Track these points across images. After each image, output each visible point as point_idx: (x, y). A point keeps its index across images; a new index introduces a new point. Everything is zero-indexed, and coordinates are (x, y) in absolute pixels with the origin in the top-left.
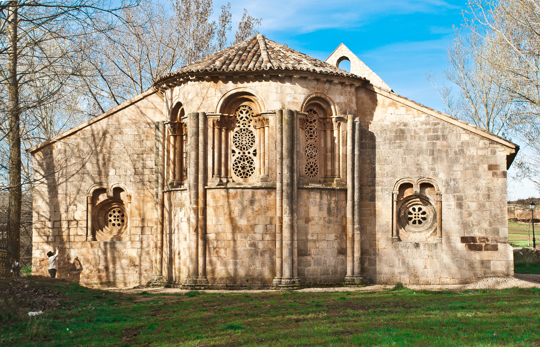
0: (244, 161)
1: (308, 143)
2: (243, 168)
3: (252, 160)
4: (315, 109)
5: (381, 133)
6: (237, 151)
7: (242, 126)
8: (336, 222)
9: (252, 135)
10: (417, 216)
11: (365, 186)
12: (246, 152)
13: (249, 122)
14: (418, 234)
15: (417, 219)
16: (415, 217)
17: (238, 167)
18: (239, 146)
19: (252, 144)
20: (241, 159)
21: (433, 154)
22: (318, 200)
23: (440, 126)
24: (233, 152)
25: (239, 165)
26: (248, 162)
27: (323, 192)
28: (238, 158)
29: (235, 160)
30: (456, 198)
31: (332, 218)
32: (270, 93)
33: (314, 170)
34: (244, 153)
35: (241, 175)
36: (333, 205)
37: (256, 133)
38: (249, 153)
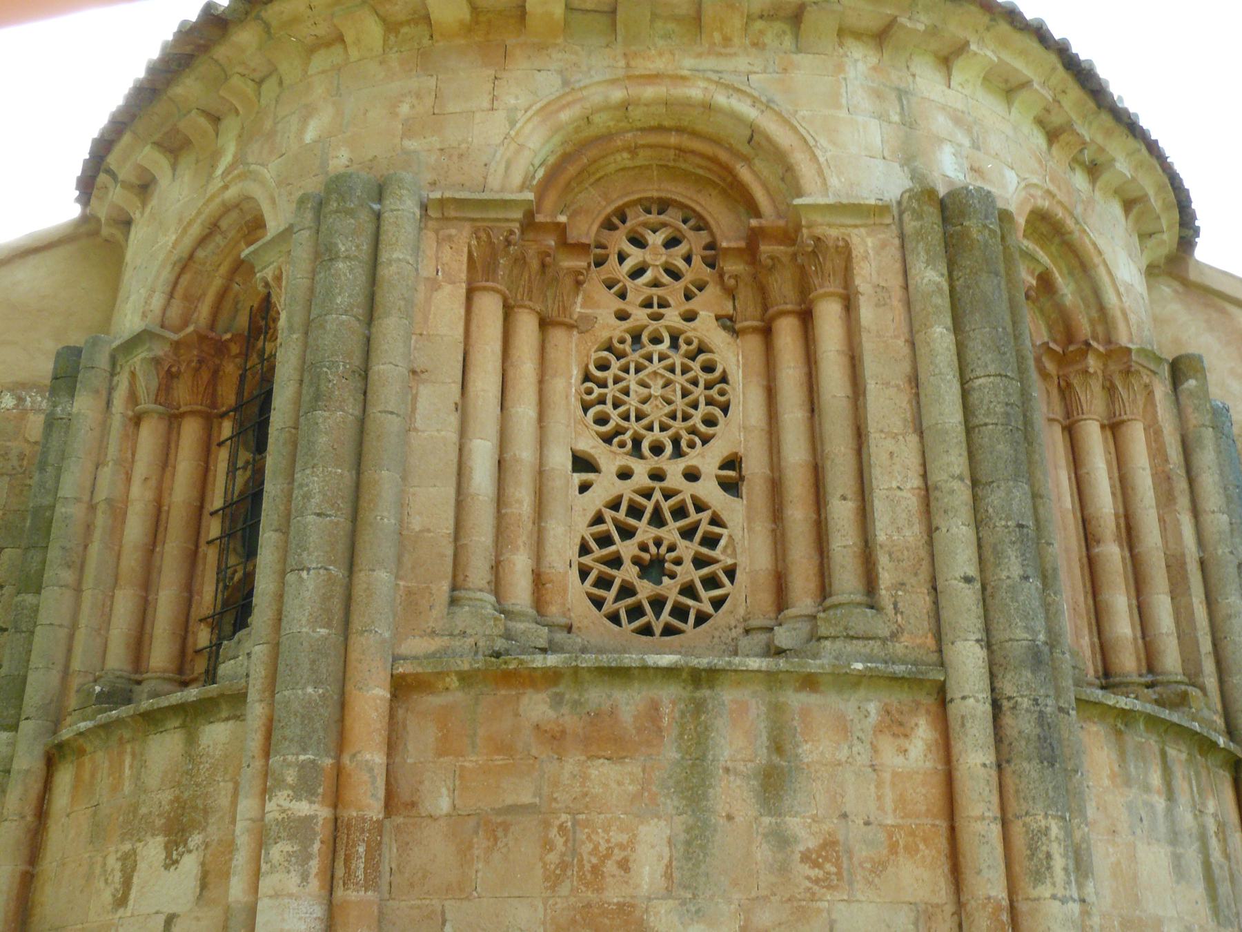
2: (652, 568)
3: (716, 521)
6: (610, 459)
7: (640, 316)
9: (708, 368)
12: (674, 471)
13: (688, 297)
18: (619, 432)
19: (710, 422)
20: (635, 511)
24: (583, 463)
25: (627, 549)
28: (615, 505)
29: (598, 519)
32: (843, 114)
34: (657, 476)
37: (731, 355)
38: (692, 476)
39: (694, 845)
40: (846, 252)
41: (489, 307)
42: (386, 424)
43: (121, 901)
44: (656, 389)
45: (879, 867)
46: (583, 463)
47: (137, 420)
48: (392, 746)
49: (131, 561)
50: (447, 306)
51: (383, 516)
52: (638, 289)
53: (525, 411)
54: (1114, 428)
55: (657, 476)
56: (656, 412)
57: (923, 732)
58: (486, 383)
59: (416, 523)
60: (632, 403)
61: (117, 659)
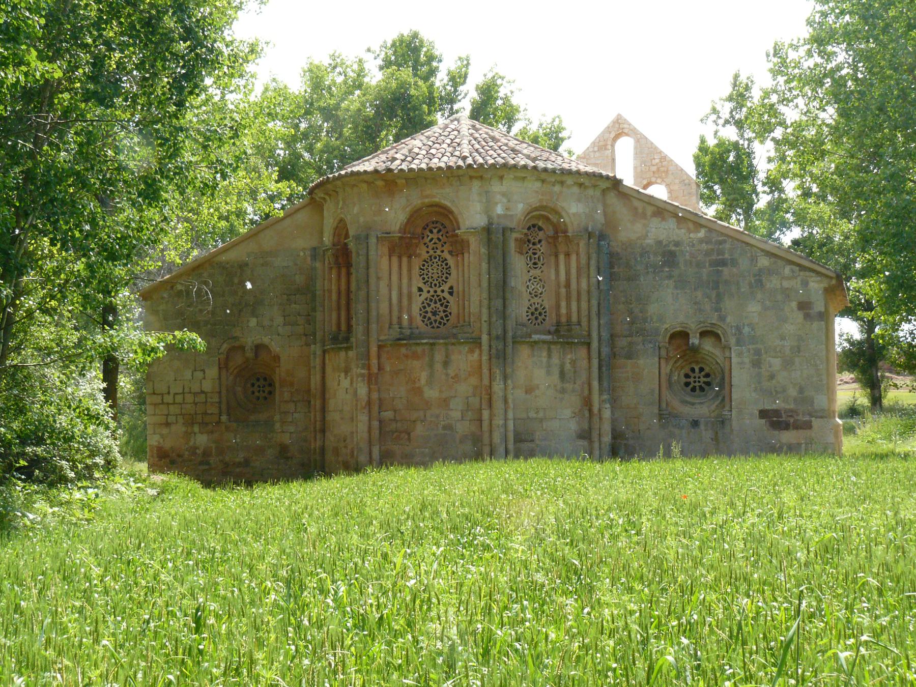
0: (436, 303)
1: (531, 274)
3: (448, 302)
4: (540, 224)
5: (642, 256)
6: (425, 288)
7: (431, 252)
8: (573, 391)
9: (447, 264)
10: (697, 379)
11: (619, 337)
12: (439, 290)
14: (698, 406)
15: (697, 384)
16: (695, 382)
17: (427, 312)
19: (447, 278)
21: (718, 287)
22: (545, 360)
23: (727, 246)
24: (420, 290)
26: (442, 305)
27: (552, 347)
30: (752, 352)
31: (567, 385)
33: (540, 314)
34: (435, 292)
35: (431, 323)
36: (568, 366)
37: (451, 261)
38: (443, 291)
39: (431, 376)
40: (468, 242)
41: (395, 260)
42: (373, 294)
43: (339, 385)
44: (435, 271)
45: (466, 379)
46: (420, 290)
47: (331, 268)
48: (379, 357)
49: (334, 304)
50: (385, 262)
51: (374, 313)
52: (431, 245)
53: (405, 281)
54: (568, 255)
55: (435, 292)
56: (435, 276)
57: (477, 352)
58: (395, 278)
59: (381, 312)
60: (430, 274)
61: (334, 328)
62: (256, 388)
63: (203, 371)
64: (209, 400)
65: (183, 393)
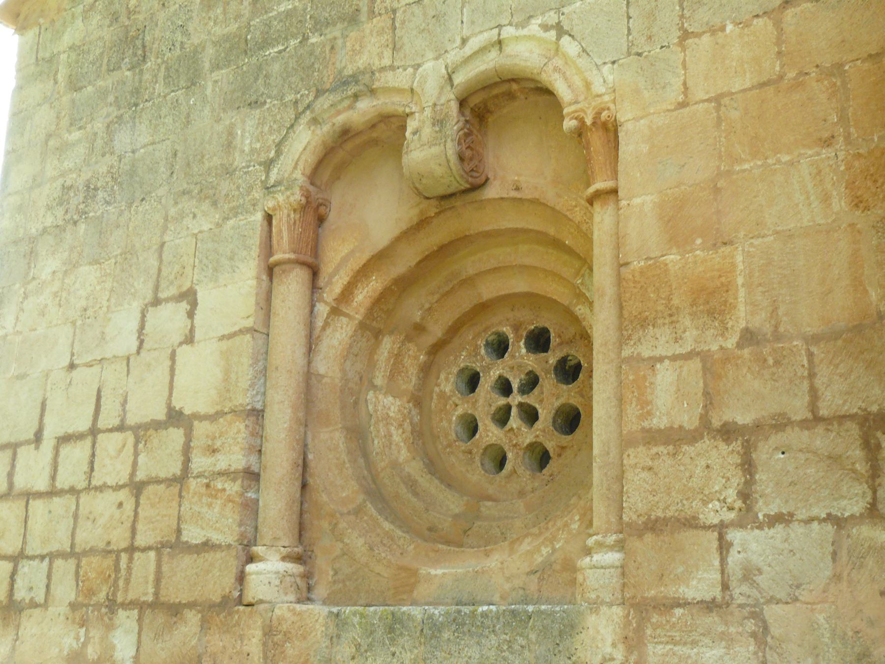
62: (486, 398)
63: (189, 297)
64: (200, 462)
65: (94, 432)
